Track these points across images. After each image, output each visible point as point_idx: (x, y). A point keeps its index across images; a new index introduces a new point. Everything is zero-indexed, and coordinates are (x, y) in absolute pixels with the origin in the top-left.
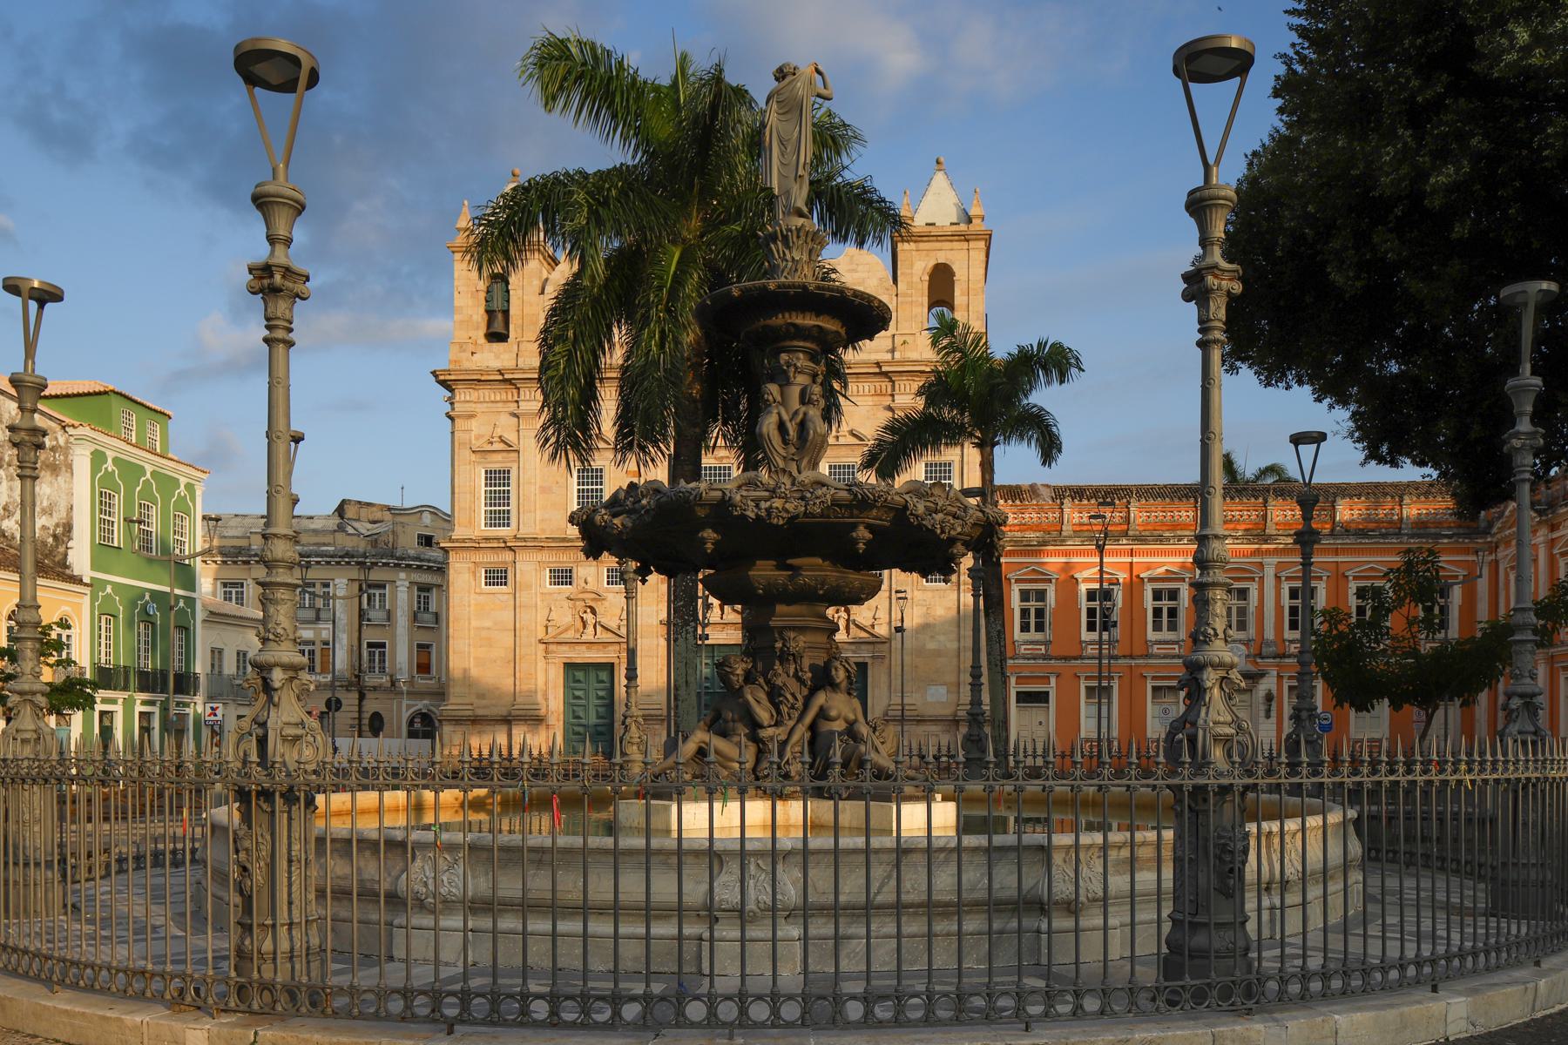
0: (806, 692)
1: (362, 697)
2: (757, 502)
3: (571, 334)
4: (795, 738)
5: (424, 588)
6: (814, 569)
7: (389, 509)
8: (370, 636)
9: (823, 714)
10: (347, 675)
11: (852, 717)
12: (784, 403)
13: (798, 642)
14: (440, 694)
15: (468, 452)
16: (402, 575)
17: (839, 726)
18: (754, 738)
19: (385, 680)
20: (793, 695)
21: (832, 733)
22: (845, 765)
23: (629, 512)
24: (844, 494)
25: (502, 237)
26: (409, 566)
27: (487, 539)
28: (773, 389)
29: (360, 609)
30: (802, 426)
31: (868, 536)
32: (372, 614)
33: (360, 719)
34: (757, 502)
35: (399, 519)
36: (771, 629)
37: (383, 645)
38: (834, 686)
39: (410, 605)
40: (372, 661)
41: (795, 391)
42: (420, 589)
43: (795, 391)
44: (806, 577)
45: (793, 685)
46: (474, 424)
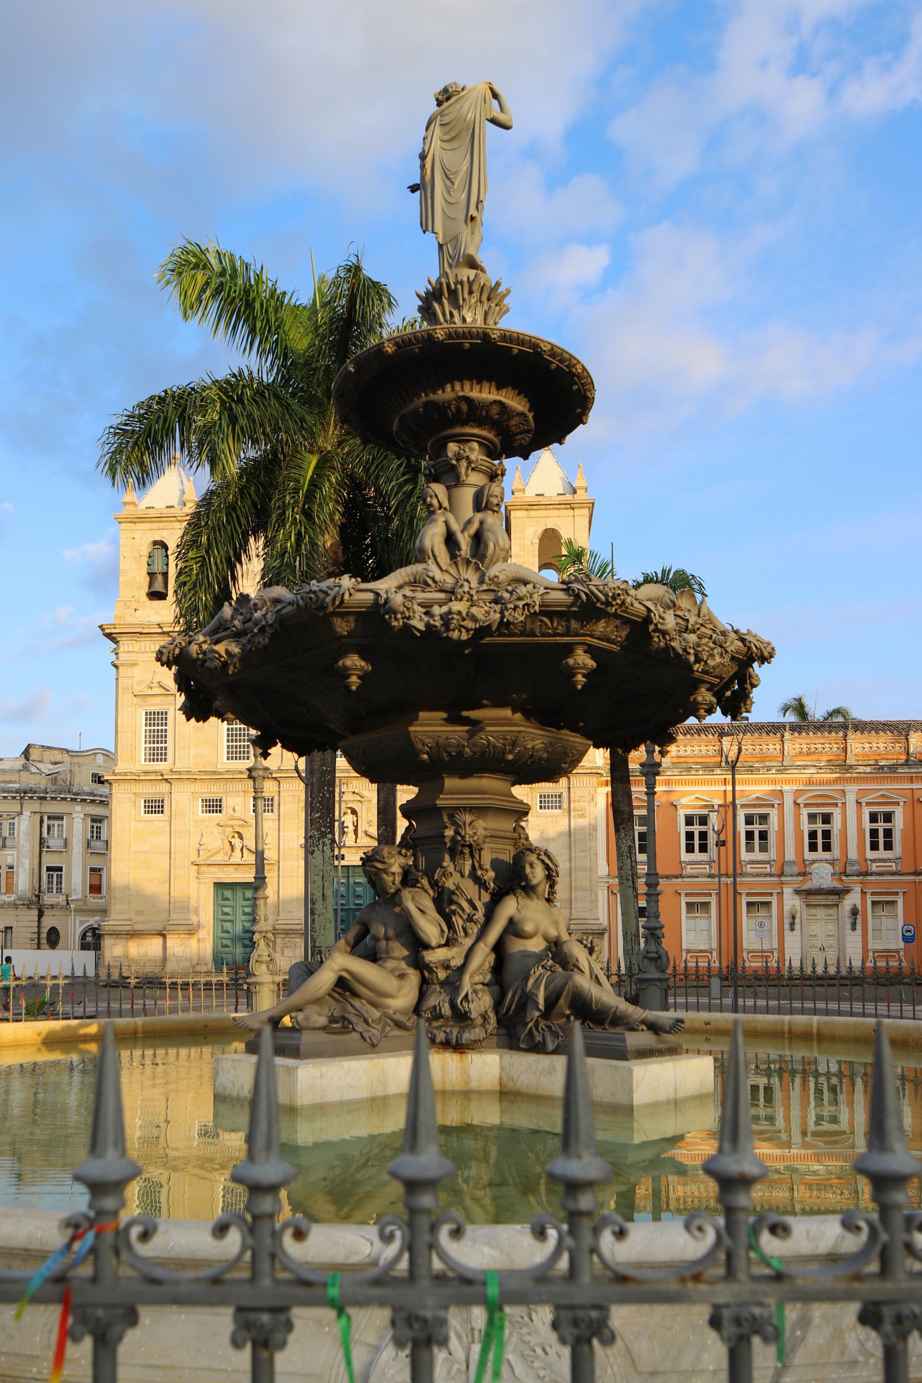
0: (486, 897)
1: (41, 914)
2: (427, 607)
3: (204, 539)
4: (475, 962)
5: (97, 820)
6: (502, 724)
7: (68, 751)
8: (50, 860)
9: (513, 929)
10: (29, 895)
11: (553, 933)
12: (452, 507)
13: (478, 829)
14: (104, 912)
15: (130, 696)
16: (78, 808)
17: (536, 945)
18: (418, 964)
19: (61, 899)
21: (526, 954)
22: (551, 1003)
23: (237, 636)
24: (560, 596)
25: (142, 442)
26: (84, 800)
27: (146, 772)
28: (439, 489)
29: (41, 838)
30: (478, 539)
31: (591, 663)
32: (51, 842)
33: (39, 933)
34: (427, 607)
35: (76, 760)
36: (438, 811)
37: (60, 869)
38: (529, 889)
39: (84, 834)
40: (50, 882)
41: (467, 495)
42: (93, 821)
43: (467, 495)
44: (491, 735)
45: (470, 888)
46: (136, 671)
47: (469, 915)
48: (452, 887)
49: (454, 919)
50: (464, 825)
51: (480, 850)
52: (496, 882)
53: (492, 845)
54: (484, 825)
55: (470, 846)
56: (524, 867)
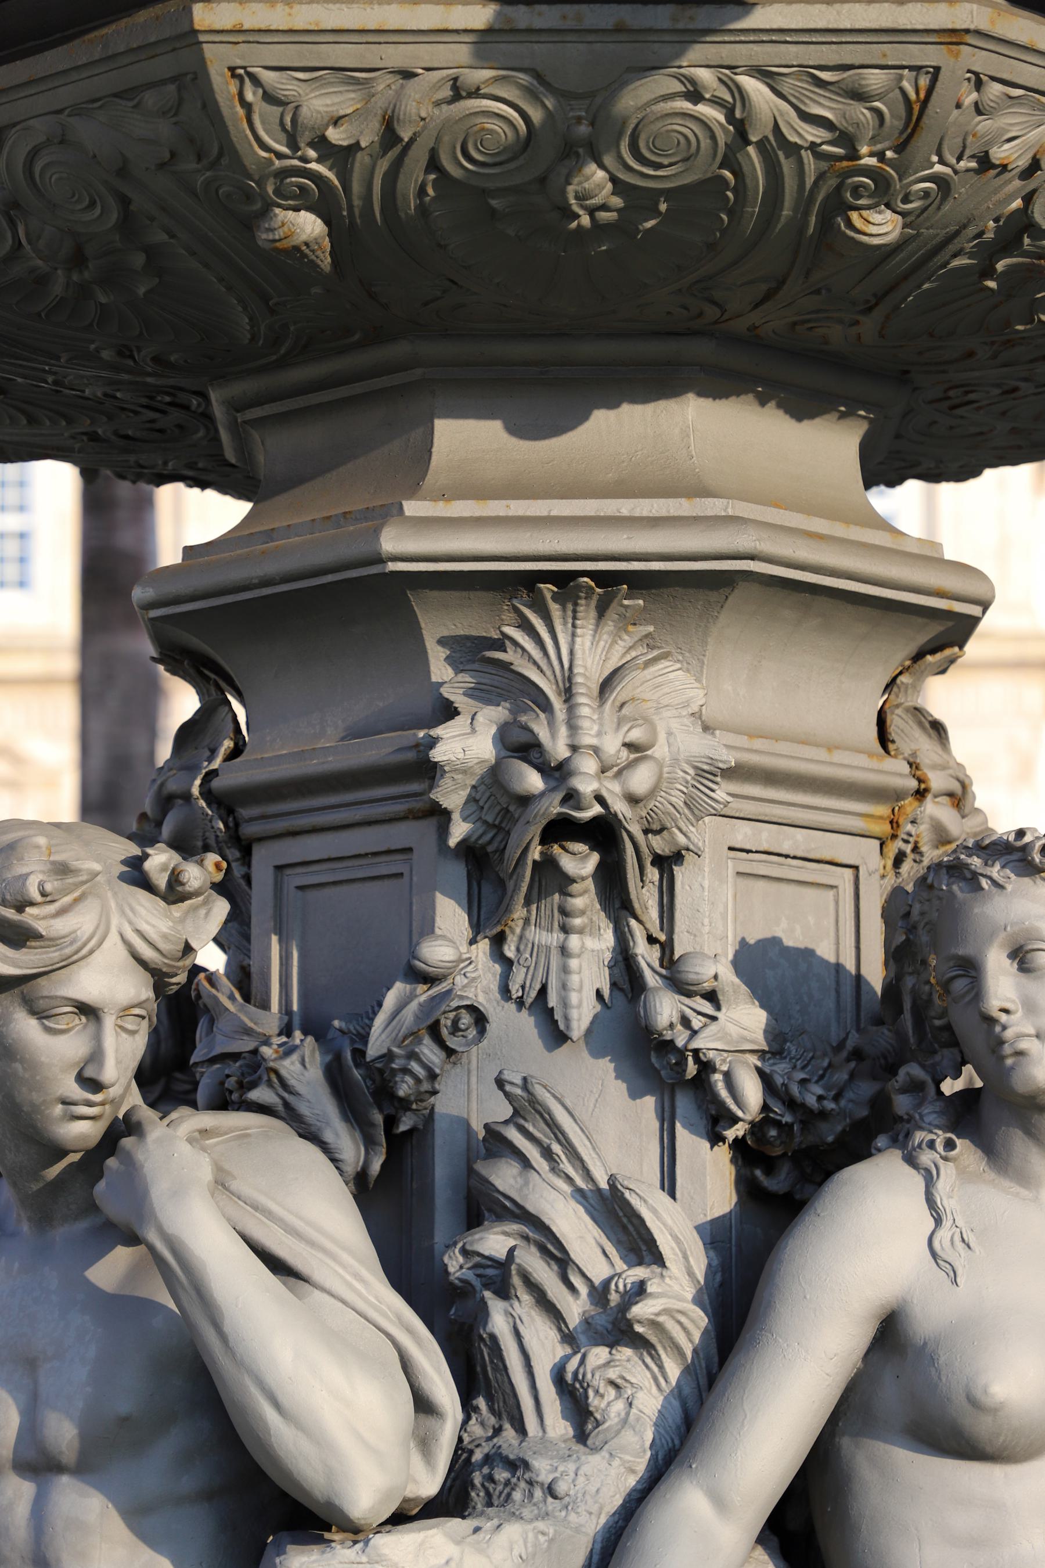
20: (614, 1212)
45: (612, 1124)
47: (600, 1293)
48: (490, 1109)
49: (498, 1322)
50: (568, 693)
51: (667, 863)
52: (780, 1070)
53: (743, 834)
54: (696, 696)
55: (603, 834)
56: (970, 969)
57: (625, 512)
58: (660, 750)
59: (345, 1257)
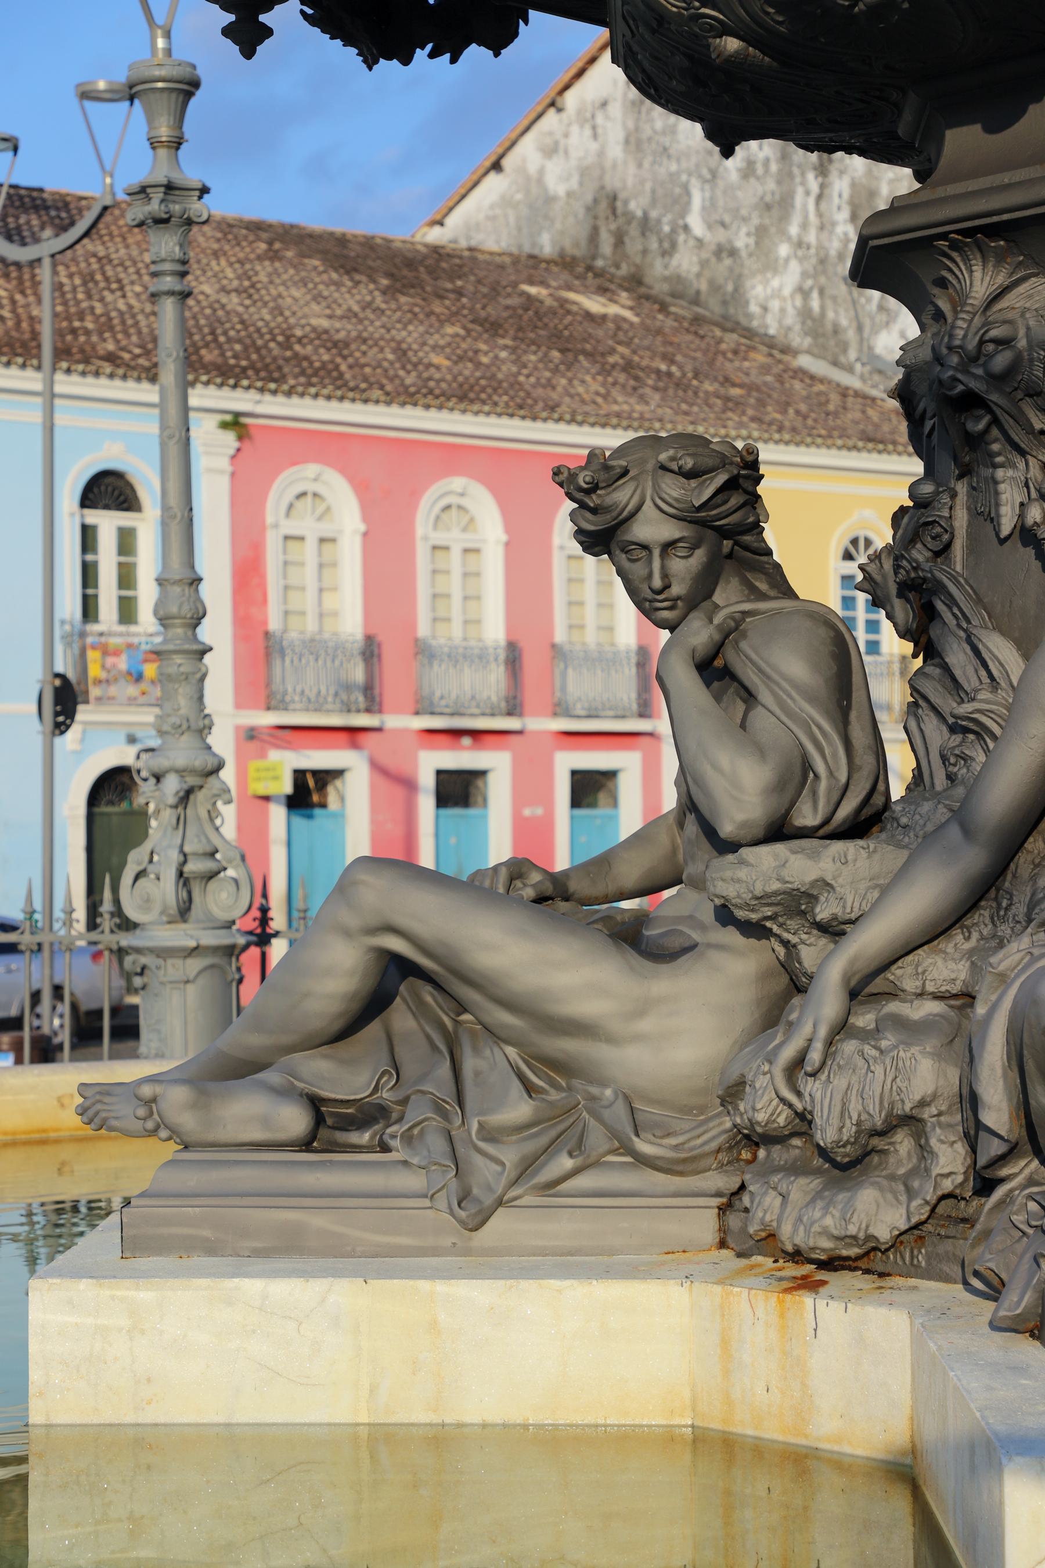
57: (1006, 181)
58: (1022, 343)
59: (784, 684)
